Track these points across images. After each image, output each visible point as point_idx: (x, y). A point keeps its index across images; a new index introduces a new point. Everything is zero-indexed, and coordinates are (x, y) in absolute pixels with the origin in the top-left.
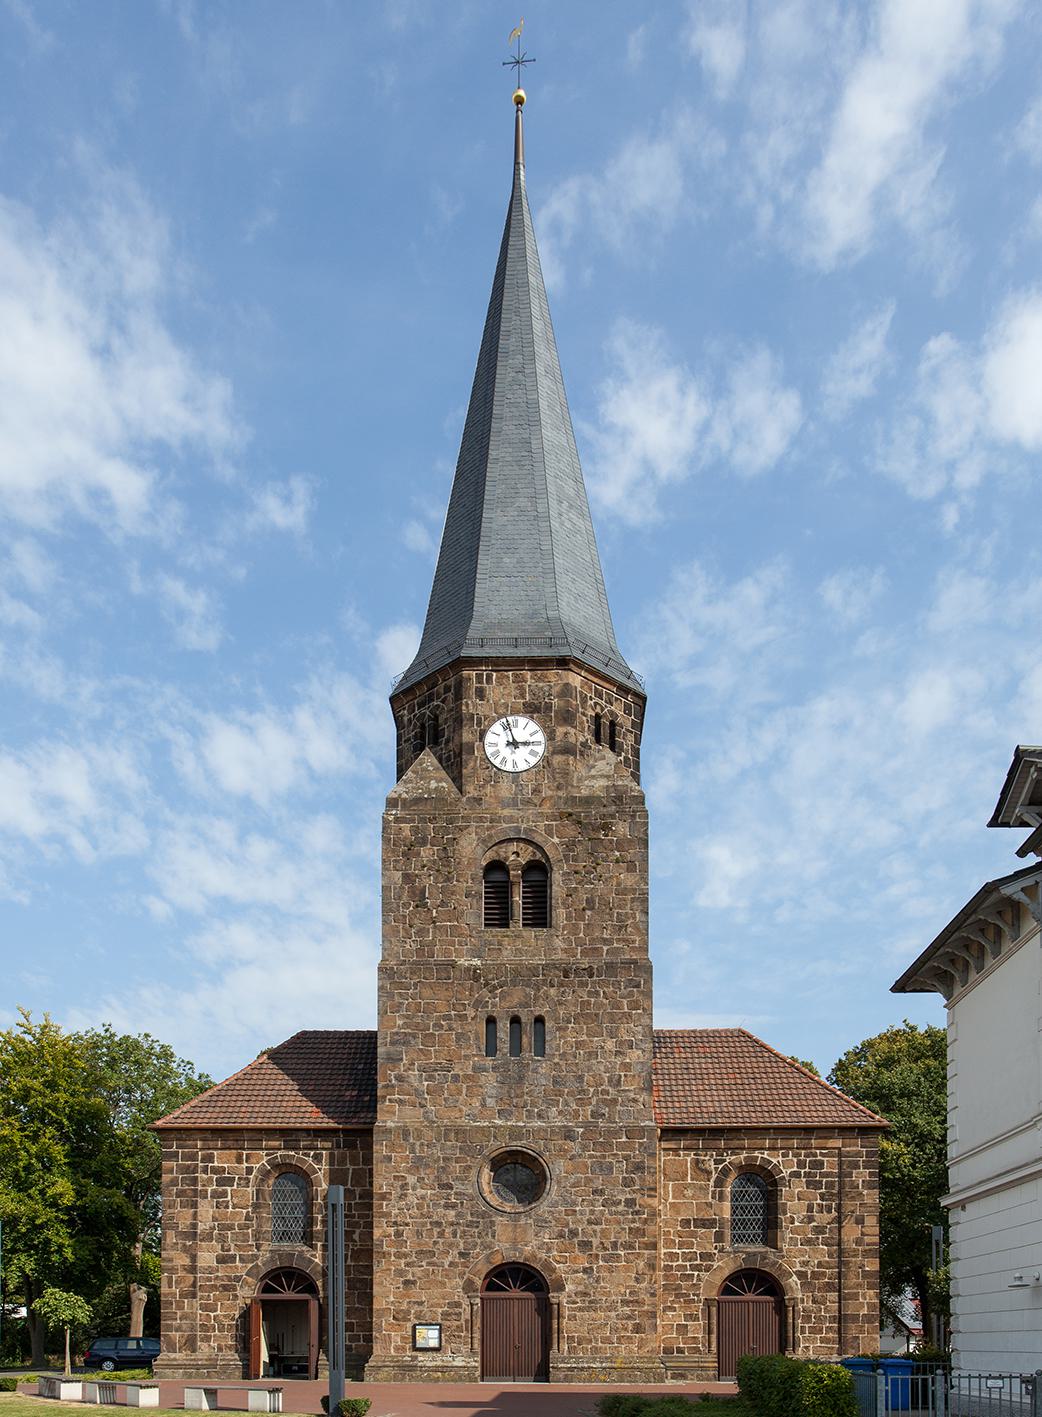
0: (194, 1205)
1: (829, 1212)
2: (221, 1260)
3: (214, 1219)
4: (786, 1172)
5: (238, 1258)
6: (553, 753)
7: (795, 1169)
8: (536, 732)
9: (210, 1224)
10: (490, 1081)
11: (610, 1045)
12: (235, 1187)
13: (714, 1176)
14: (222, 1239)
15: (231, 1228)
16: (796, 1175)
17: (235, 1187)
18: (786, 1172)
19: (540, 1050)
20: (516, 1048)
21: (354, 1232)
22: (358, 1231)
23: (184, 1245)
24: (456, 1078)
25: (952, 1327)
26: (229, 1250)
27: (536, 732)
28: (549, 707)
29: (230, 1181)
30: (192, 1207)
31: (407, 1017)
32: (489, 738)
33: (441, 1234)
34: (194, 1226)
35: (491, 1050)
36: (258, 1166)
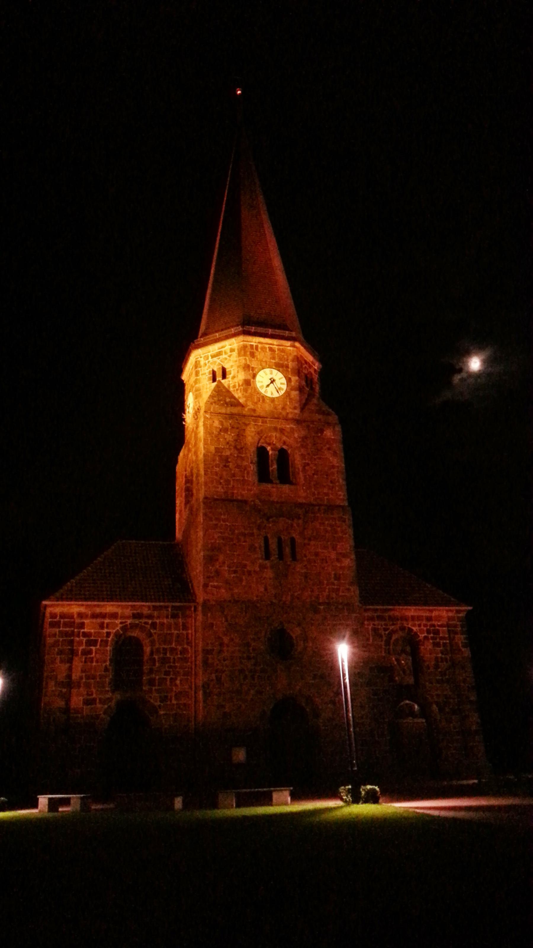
0: (70, 661)
1: (447, 662)
2: (87, 702)
3: (82, 671)
4: (422, 636)
5: (98, 701)
6: (292, 389)
7: (426, 634)
8: (282, 378)
9: (79, 674)
10: (269, 574)
11: (333, 556)
12: (98, 647)
13: (384, 638)
14: (88, 686)
15: (94, 678)
16: (426, 638)
17: (98, 647)
18: (422, 636)
19: (294, 557)
20: (281, 556)
21: (176, 679)
22: (179, 678)
23: (61, 691)
24: (249, 573)
25: (283, 791)
26: (92, 695)
27: (282, 378)
28: (287, 367)
29: (95, 643)
30: (68, 662)
31: (221, 533)
32: (258, 378)
33: (245, 677)
34: (69, 676)
35: (267, 556)
36: (114, 631)
